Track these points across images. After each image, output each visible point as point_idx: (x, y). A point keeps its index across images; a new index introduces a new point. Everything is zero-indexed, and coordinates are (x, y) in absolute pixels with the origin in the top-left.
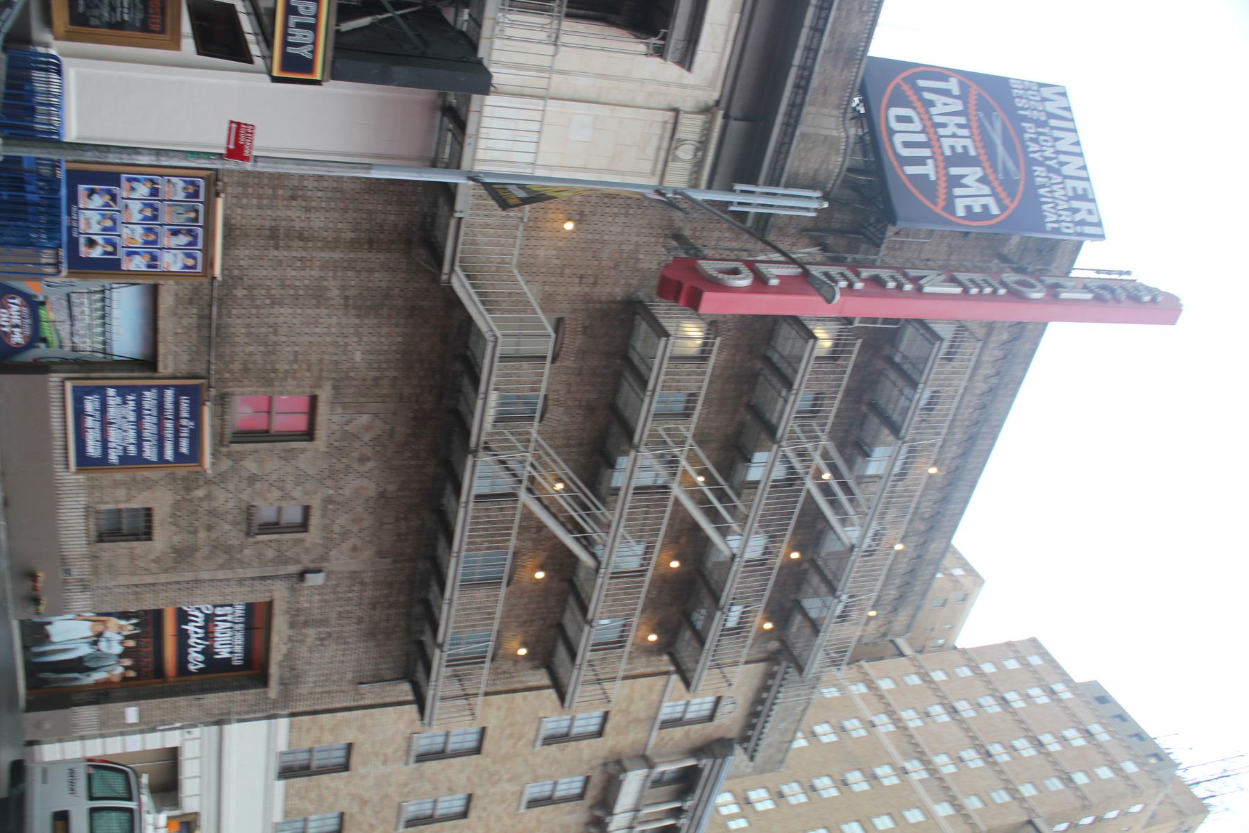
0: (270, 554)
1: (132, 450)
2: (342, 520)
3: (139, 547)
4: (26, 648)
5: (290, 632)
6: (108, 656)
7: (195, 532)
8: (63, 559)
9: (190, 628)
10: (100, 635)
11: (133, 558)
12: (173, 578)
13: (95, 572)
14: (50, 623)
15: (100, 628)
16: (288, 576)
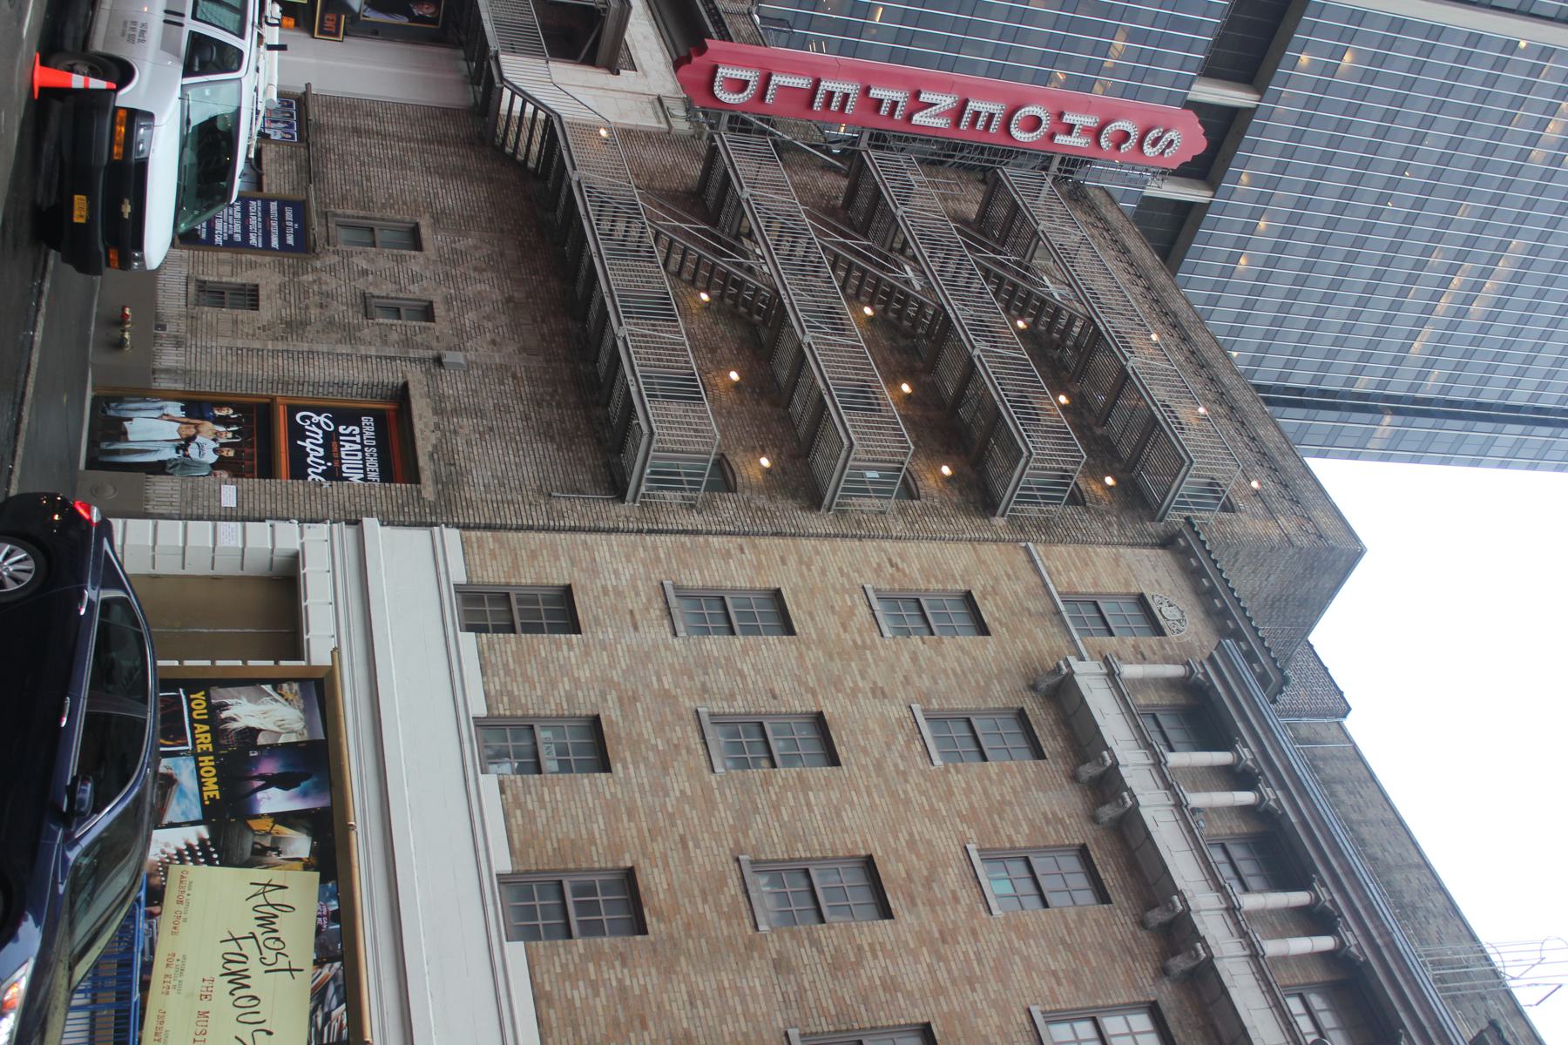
0: (394, 336)
1: (238, 238)
2: (470, 317)
3: (244, 315)
4: (93, 443)
5: (436, 419)
6: (199, 465)
7: (307, 307)
8: (157, 316)
9: (308, 444)
10: (190, 439)
11: (235, 322)
12: (280, 346)
13: (193, 331)
14: (130, 419)
15: (192, 431)
16: (422, 361)
